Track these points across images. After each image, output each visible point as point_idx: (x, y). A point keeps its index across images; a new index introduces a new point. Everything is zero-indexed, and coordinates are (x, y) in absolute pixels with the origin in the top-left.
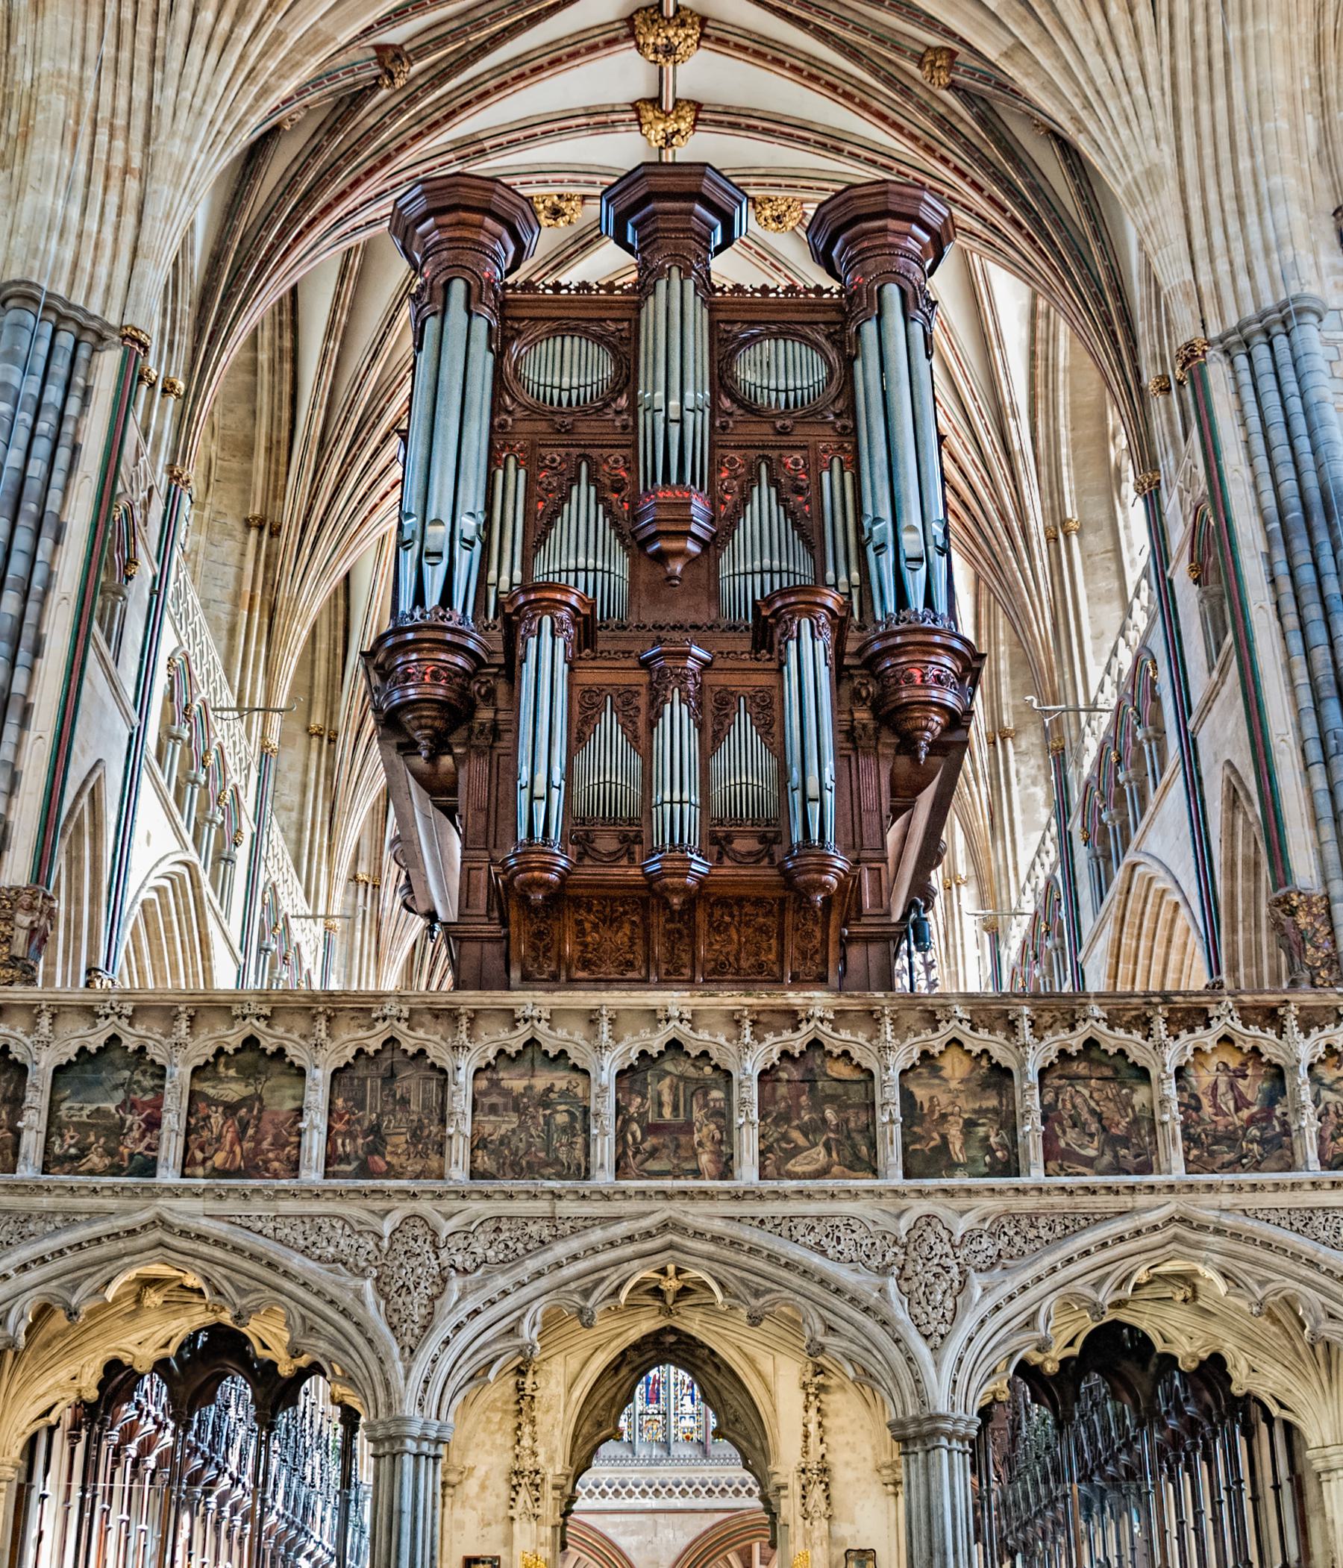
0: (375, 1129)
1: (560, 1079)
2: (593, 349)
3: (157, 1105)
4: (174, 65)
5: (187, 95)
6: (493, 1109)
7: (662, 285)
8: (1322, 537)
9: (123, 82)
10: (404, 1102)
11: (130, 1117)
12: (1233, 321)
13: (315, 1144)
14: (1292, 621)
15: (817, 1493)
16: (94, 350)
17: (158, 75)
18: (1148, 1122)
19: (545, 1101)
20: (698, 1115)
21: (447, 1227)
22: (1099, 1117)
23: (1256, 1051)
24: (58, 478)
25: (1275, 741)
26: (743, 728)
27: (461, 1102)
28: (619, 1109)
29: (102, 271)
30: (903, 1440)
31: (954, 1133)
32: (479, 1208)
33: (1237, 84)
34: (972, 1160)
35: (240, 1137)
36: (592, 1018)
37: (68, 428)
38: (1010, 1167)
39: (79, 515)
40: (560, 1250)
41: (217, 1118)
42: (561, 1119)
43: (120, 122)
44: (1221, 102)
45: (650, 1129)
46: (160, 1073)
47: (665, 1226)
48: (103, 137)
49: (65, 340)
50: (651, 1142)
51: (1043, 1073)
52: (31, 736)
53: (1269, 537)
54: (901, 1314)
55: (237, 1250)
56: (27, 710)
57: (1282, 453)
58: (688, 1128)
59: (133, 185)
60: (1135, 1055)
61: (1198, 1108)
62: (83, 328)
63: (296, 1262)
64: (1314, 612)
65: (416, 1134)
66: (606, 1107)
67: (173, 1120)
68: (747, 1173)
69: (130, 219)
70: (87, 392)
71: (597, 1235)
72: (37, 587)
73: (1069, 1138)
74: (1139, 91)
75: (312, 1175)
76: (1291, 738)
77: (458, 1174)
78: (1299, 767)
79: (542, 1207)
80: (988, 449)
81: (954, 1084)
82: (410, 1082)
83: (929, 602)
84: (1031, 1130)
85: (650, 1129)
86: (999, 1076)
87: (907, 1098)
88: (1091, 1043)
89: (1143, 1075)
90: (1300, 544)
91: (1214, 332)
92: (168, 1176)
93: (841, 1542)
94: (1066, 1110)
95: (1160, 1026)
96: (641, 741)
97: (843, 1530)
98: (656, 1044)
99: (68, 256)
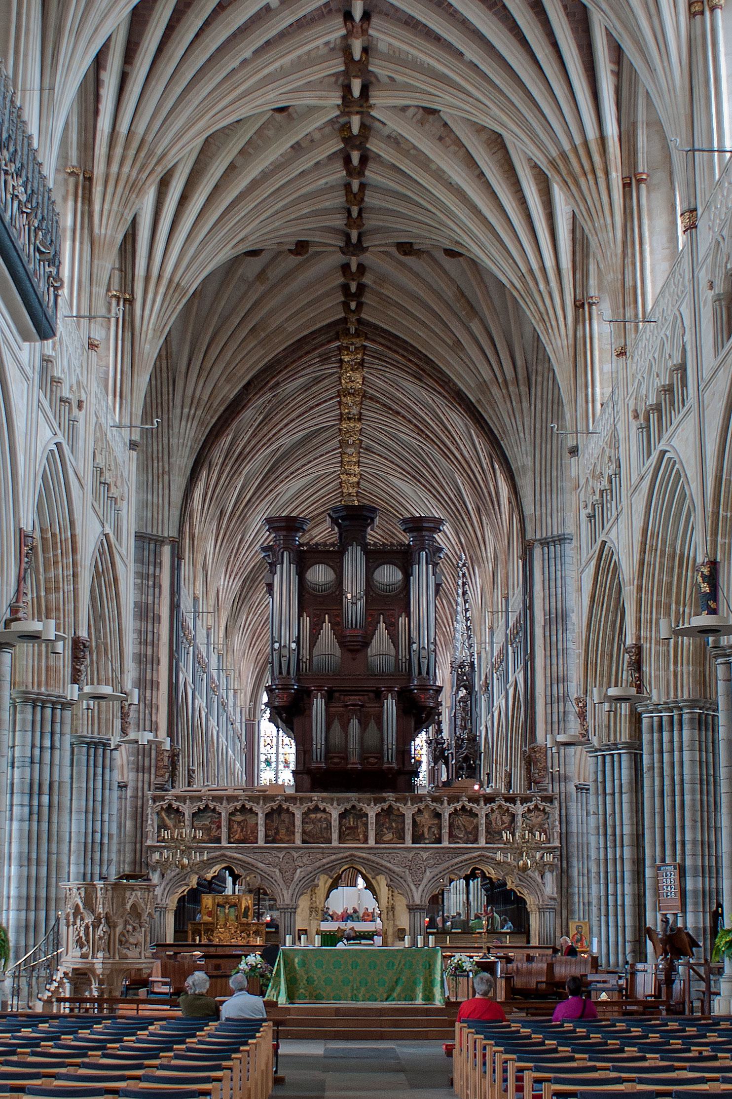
0: (276, 828)
1: (324, 816)
2: (329, 569)
3: (220, 823)
4: (176, 430)
5: (181, 441)
6: (307, 823)
7: (350, 548)
8: (560, 628)
9: (160, 440)
10: (284, 821)
11: (213, 826)
12: (544, 536)
13: (261, 834)
14: (548, 653)
15: (391, 913)
16: (161, 545)
17: (171, 432)
18: (476, 828)
19: (320, 820)
20: (359, 824)
21: (295, 855)
22: (464, 826)
23: (508, 810)
24: (156, 601)
25: (537, 694)
26: (372, 724)
27: (298, 822)
28: (340, 823)
29: (160, 516)
30: (410, 909)
31: (426, 830)
32: (303, 851)
33: (555, 442)
34: (430, 838)
35: (242, 831)
36: (332, 799)
37: (157, 581)
38: (439, 841)
39: (165, 612)
40: (324, 861)
41: (235, 826)
42: (324, 826)
43: (160, 455)
44: (549, 446)
45: (347, 828)
46: (220, 814)
47: (351, 855)
48: (155, 465)
49: (152, 546)
50: (348, 831)
51: (450, 815)
52: (161, 692)
53: (545, 620)
54: (409, 879)
55: (244, 862)
56: (158, 683)
57: (553, 591)
58: (357, 828)
59: (166, 477)
60: (474, 810)
61: (491, 824)
62: (157, 541)
63: (260, 865)
64: (554, 653)
65: (287, 829)
66: (335, 823)
67: (224, 830)
68: (372, 842)
69: (166, 492)
70: (161, 563)
71: (334, 857)
72: (155, 642)
73: (456, 832)
74: (522, 435)
75: (261, 843)
76: (543, 694)
77: (298, 842)
78: (544, 704)
79: (320, 850)
80: (485, 466)
81: (427, 816)
82: (285, 816)
83: (428, 673)
84: (445, 831)
85: (347, 828)
86: (438, 816)
87: (414, 821)
88: (463, 807)
89: (477, 815)
90: (554, 627)
91: (538, 537)
92: (224, 844)
93: (397, 926)
94: (456, 824)
95: (482, 803)
96: (345, 727)
97: (398, 923)
98: (349, 807)
99: (150, 515)
